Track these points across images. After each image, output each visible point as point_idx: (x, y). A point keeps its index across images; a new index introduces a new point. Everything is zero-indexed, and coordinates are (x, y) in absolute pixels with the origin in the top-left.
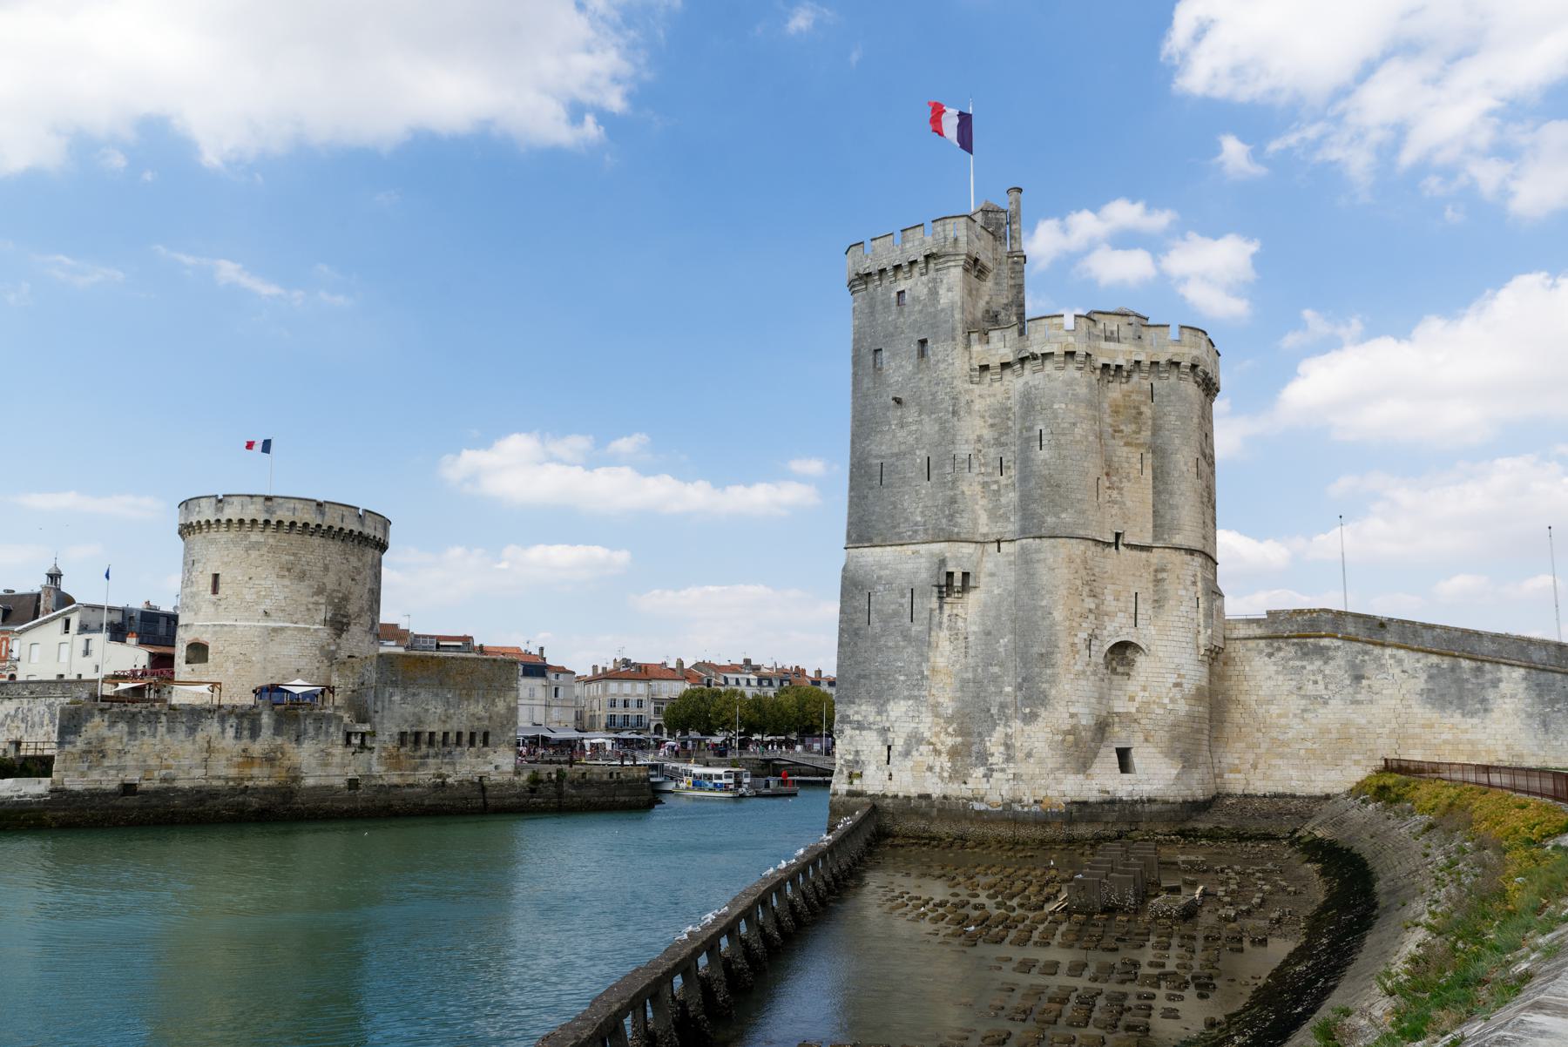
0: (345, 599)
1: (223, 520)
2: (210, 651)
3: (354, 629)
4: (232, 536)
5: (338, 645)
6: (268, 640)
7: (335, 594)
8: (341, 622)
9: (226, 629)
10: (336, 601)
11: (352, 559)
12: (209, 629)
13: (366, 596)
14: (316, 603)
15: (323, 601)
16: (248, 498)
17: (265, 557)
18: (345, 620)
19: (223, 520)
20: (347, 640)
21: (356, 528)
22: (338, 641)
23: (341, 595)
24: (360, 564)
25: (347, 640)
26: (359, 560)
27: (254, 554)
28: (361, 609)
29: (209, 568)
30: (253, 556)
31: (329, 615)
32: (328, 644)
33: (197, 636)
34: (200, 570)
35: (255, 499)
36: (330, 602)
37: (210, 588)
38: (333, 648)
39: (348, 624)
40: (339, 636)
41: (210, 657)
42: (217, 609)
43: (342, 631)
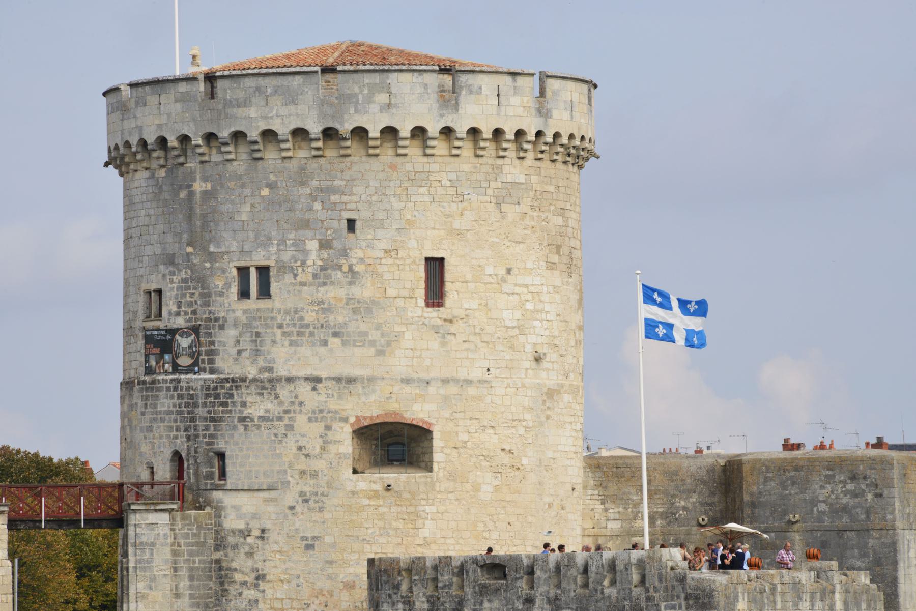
1: (461, 130)
2: (437, 442)
4: (466, 168)
6: (543, 419)
9: (472, 391)
12: (432, 389)
16: (508, 79)
17: (528, 222)
19: (461, 130)
27: (513, 211)
29: (413, 243)
30: (510, 217)
33: (393, 406)
34: (384, 245)
35: (520, 80)
37: (421, 292)
41: (437, 457)
42: (443, 344)
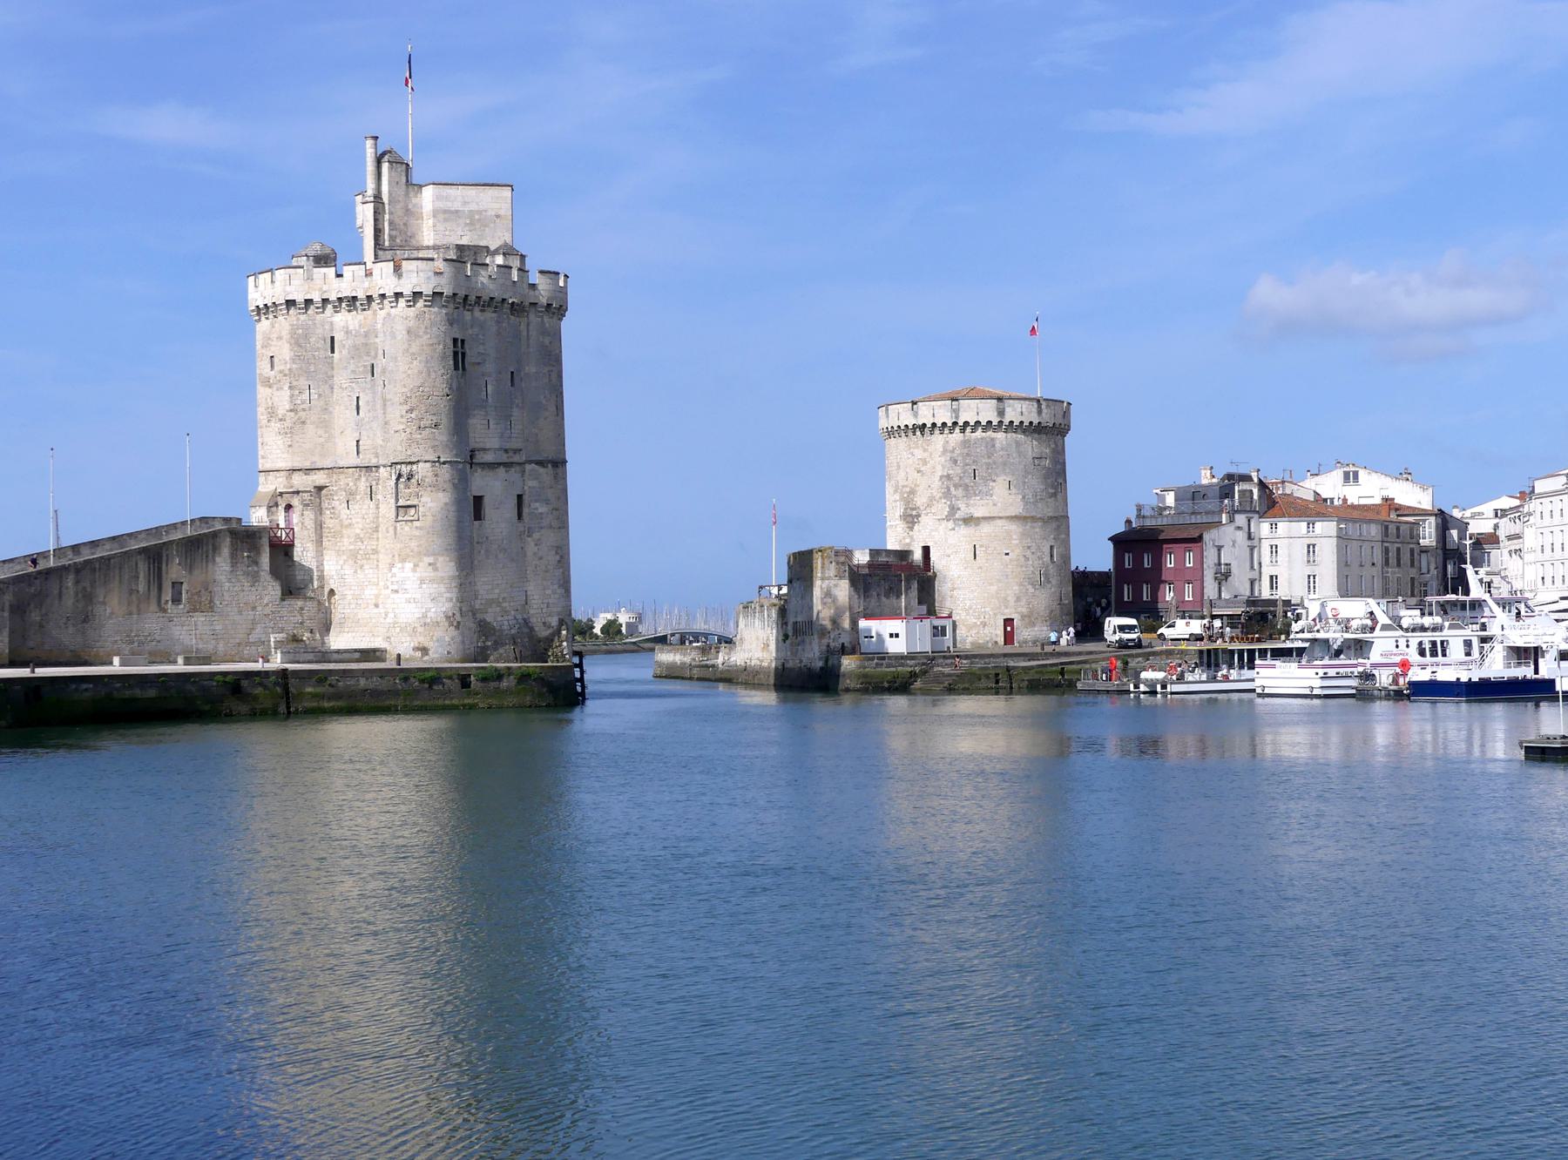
0: (912, 492)
3: (923, 519)
5: (912, 537)
7: (904, 490)
8: (911, 515)
10: (905, 495)
11: (916, 452)
13: (937, 483)
14: (895, 501)
15: (898, 498)
18: (914, 513)
20: (919, 531)
21: (910, 422)
22: (911, 533)
23: (908, 490)
24: (926, 455)
25: (919, 531)
26: (925, 450)
28: (932, 499)
31: (902, 510)
32: (904, 538)
36: (902, 498)
38: (908, 541)
39: (920, 516)
40: (911, 529)
43: (913, 523)
